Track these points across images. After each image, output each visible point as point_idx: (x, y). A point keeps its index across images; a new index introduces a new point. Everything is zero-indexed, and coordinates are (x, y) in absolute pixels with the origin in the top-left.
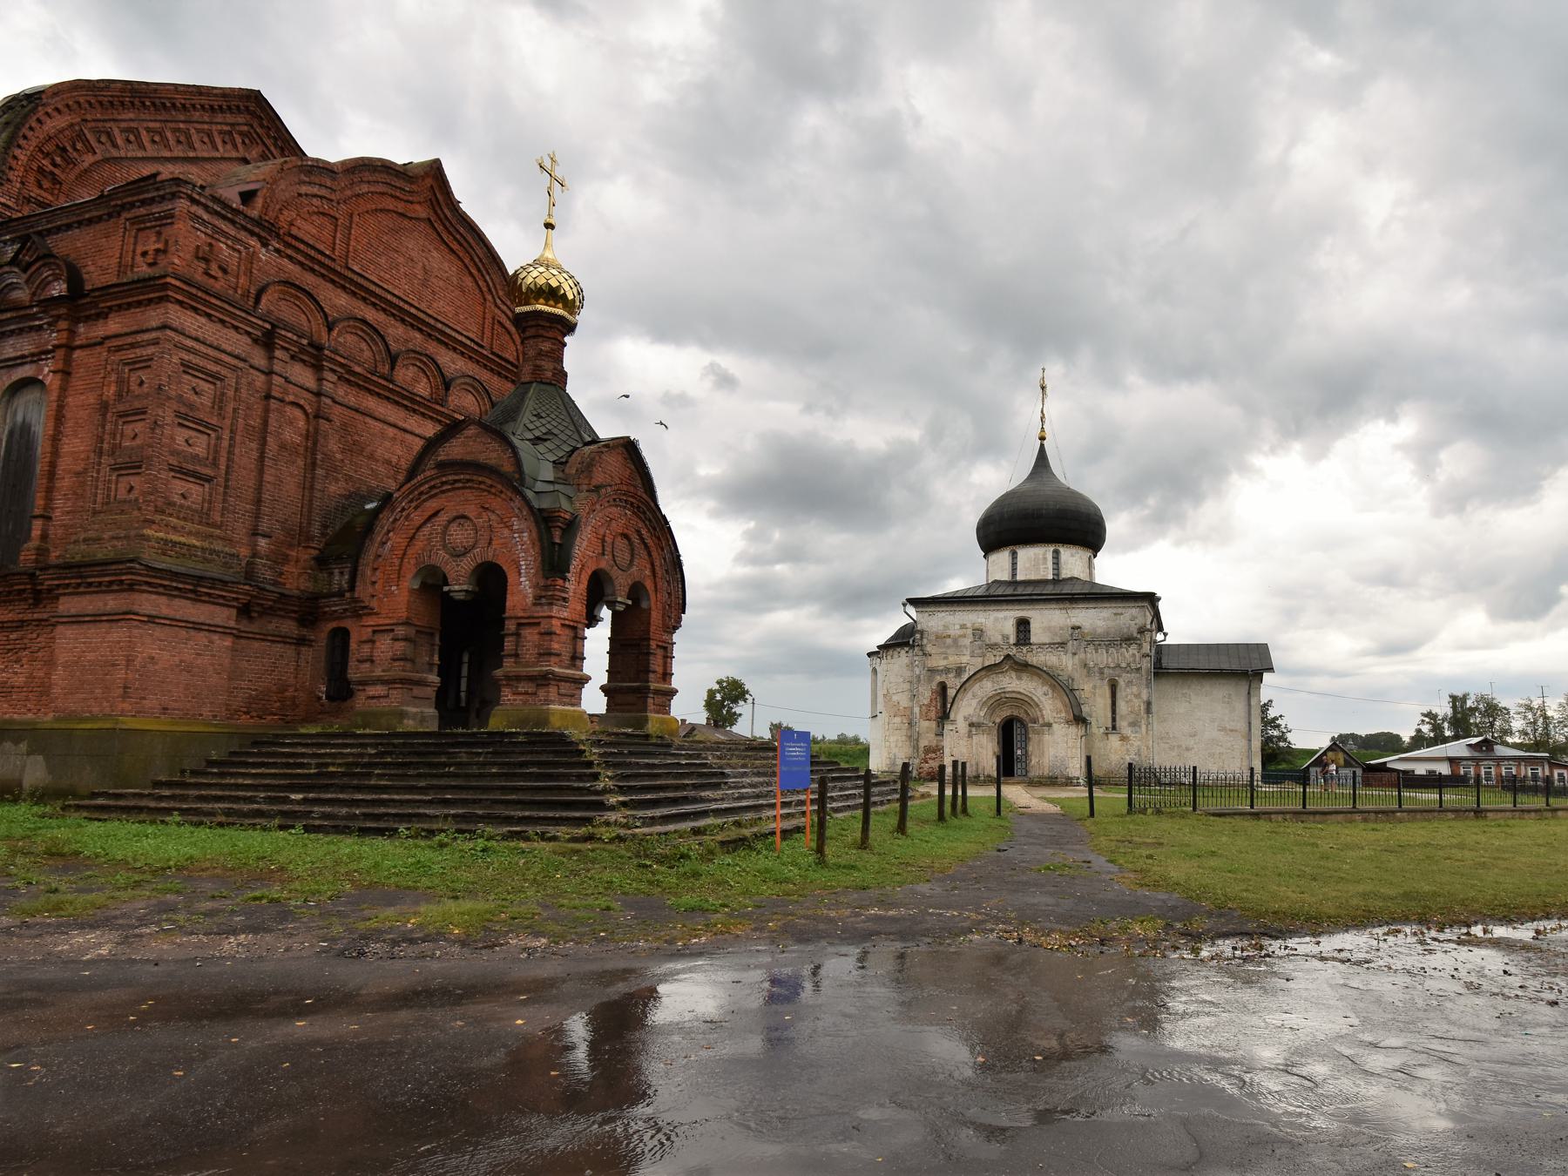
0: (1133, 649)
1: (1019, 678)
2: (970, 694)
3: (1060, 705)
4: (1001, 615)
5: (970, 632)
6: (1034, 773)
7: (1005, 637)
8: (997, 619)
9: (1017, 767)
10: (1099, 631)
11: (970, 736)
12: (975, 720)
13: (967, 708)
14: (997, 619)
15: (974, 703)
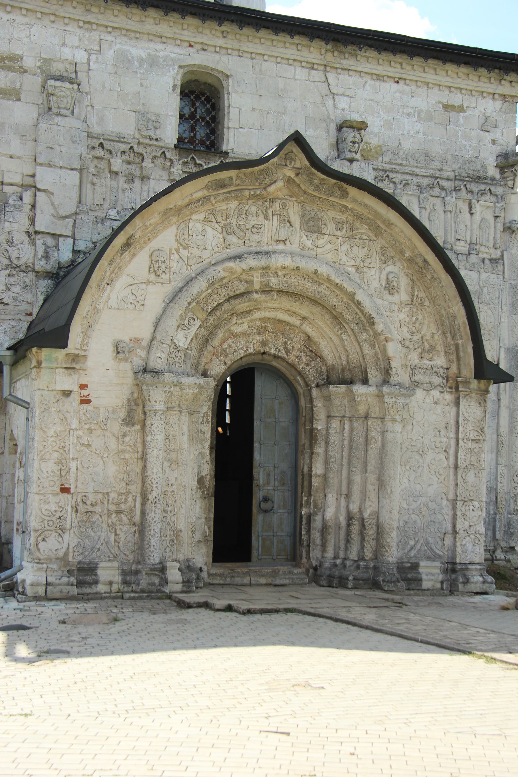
0: (483, 208)
1: (313, 226)
2: (138, 264)
3: (429, 329)
4: (139, 50)
5: (31, 84)
6: (325, 553)
7: (149, 121)
8: (123, 62)
9: (267, 528)
10: (408, 145)
11: (136, 413)
12: (158, 359)
13: (120, 312)
14: (123, 62)
15: (155, 297)
